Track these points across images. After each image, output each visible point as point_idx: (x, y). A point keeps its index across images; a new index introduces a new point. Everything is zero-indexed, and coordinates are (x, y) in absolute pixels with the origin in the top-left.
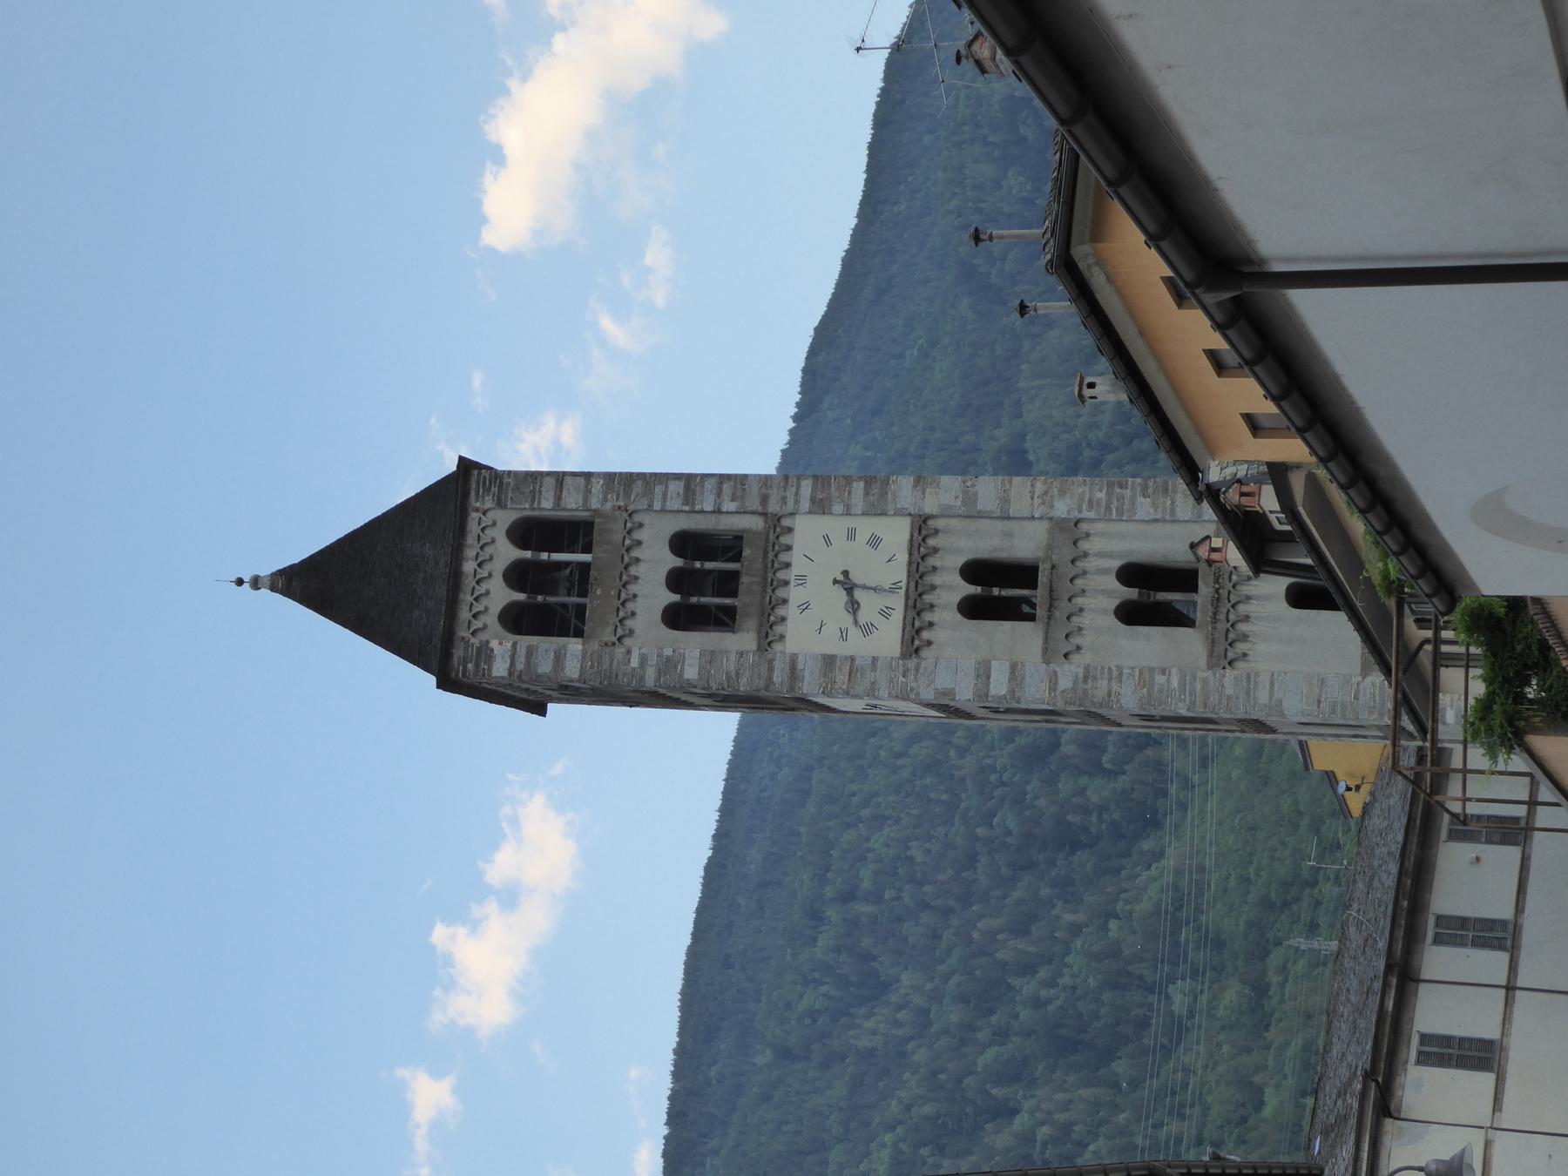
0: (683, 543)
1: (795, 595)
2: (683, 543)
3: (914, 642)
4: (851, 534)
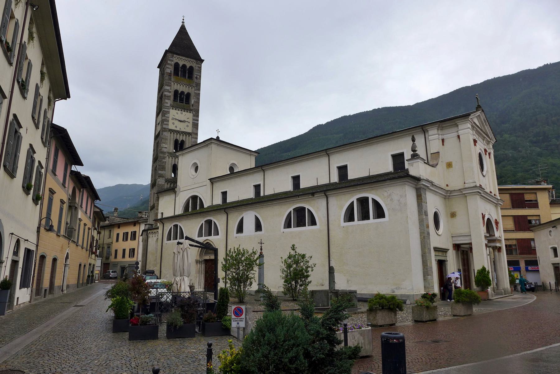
0: (188, 95)
1: (179, 112)
2: (188, 95)
3: (171, 131)
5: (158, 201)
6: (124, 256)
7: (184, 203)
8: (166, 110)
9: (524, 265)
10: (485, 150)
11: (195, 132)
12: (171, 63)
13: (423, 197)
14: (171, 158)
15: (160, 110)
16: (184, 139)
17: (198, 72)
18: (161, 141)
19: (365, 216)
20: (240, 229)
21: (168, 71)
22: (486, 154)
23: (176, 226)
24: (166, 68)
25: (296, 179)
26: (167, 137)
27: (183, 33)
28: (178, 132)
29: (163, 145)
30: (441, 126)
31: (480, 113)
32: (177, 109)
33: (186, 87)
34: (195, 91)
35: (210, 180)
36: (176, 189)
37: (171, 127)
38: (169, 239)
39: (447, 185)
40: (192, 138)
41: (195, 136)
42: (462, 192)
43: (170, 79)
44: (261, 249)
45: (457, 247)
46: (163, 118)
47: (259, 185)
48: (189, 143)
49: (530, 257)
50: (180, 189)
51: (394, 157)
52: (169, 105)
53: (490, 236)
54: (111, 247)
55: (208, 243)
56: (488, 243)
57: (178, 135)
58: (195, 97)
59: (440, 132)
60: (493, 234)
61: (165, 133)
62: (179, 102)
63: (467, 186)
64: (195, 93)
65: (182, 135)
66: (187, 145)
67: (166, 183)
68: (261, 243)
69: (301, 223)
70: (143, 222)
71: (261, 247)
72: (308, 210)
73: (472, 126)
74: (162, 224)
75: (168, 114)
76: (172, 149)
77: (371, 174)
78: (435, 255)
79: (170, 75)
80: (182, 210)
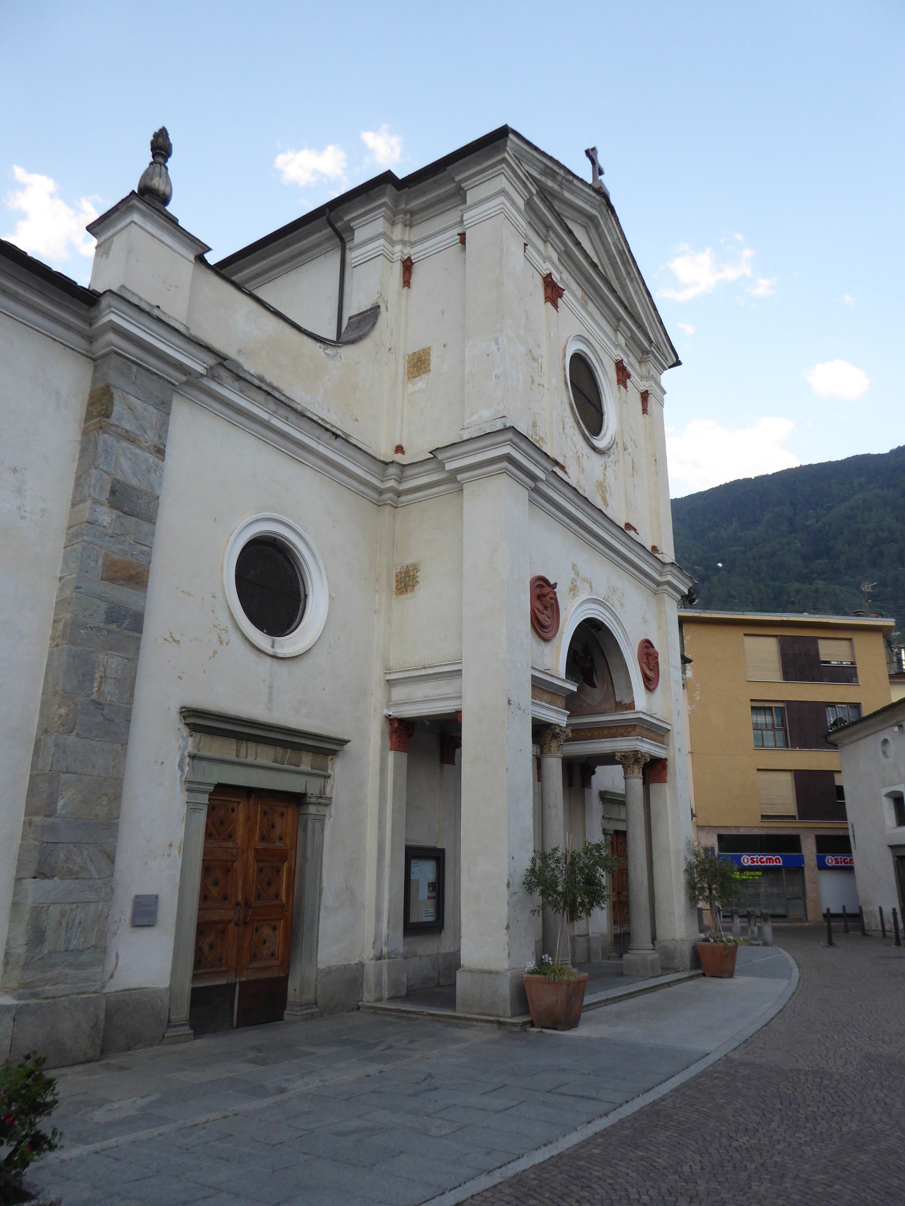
9: (814, 850)
30: (403, 206)
39: (399, 449)
42: (441, 465)
49: (827, 827)
59: (398, 232)
60: (627, 701)
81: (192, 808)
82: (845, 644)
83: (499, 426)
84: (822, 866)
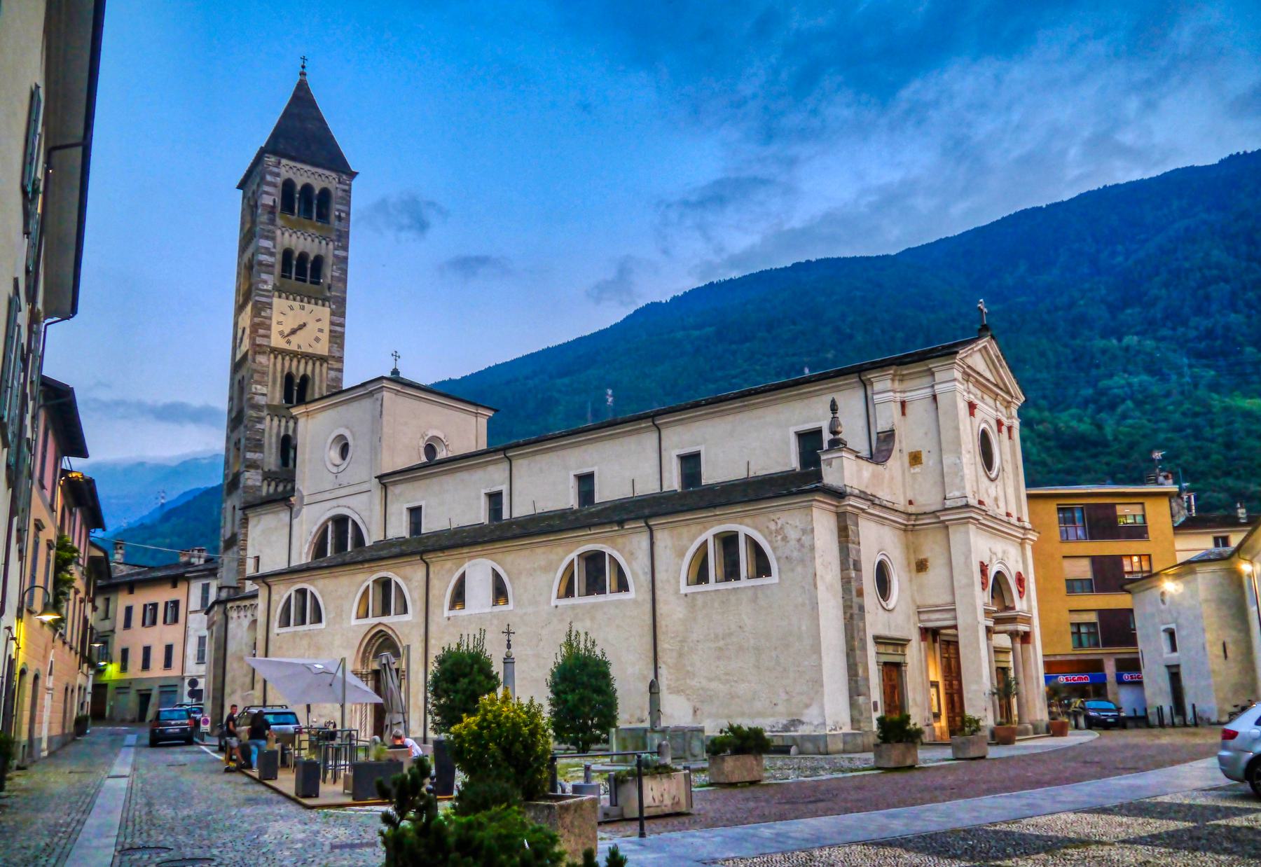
0: (319, 262)
1: (296, 304)
2: (319, 262)
3: (276, 352)
4: (321, 330)
5: (247, 527)
6: (146, 665)
7: (313, 534)
8: (264, 299)
10: (999, 423)
11: (337, 354)
12: (273, 180)
13: (850, 532)
14: (276, 420)
15: (247, 295)
16: (309, 372)
17: (341, 204)
18: (252, 377)
19: (731, 572)
20: (459, 597)
21: (268, 200)
22: (1000, 431)
23: (302, 593)
24: (261, 194)
25: (586, 482)
26: (268, 367)
27: (302, 100)
28: (294, 355)
29: (256, 388)
30: (899, 373)
31: (988, 342)
32: (291, 297)
33: (313, 241)
34: (337, 252)
35: (380, 478)
36: (292, 499)
37: (276, 341)
38: (285, 622)
40: (329, 369)
41: (336, 365)
42: (938, 517)
43: (272, 221)
44: (509, 646)
45: (929, 634)
46: (257, 320)
47: (499, 494)
48: (321, 381)
49: (1124, 652)
50: (302, 498)
51: (802, 436)
52: (270, 287)
53: (1007, 608)
54: (110, 641)
55: (381, 631)
56: (995, 624)
57: (295, 362)
58: (335, 267)
59: (897, 385)
60: (1011, 606)
61: (262, 359)
62: (297, 279)
63: (949, 504)
64: (336, 256)
65: (303, 361)
66: (318, 388)
67: (266, 482)
68: (509, 633)
69: (595, 585)
70: (196, 578)
71: (509, 641)
72: (610, 556)
73: (965, 373)
74: (267, 589)
75: (268, 311)
76: (277, 397)
77: (752, 474)
78: (877, 653)
79: (272, 210)
80: (309, 549)
81: (879, 670)
82: (1139, 507)
83: (961, 503)
84: (1120, 681)
